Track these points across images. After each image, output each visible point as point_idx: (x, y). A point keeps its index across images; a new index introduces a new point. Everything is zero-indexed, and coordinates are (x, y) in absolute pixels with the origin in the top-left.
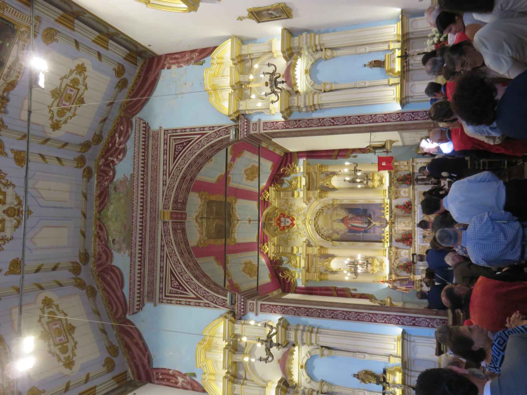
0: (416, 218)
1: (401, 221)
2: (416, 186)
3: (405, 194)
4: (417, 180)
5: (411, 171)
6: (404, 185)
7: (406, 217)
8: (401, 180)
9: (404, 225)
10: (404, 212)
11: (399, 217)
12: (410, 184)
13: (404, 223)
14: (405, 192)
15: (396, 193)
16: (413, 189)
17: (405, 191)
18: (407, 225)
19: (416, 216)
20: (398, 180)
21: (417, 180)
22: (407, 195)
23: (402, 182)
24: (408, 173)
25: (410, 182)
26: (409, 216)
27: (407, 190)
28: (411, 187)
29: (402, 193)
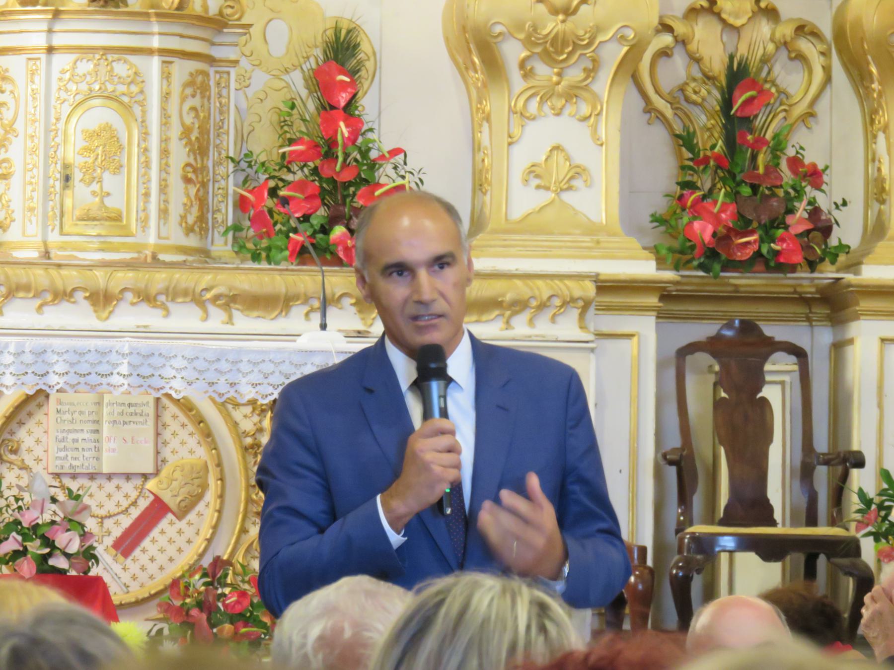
0: (184, 317)
1: (127, 104)
2: (644, 336)
3: (533, 172)
4: (741, 356)
5: (872, 273)
6: (661, 172)
7: (196, 176)
8: (736, 124)
9: (72, 151)
10: (265, 145)
11: (198, 86)
12: (680, 253)
13: (108, 149)
14: (559, 176)
15: (555, 50)
16: (606, 287)
17: (578, 171)
18: (82, 195)
19: (216, 320)
20: (738, 75)
21: (741, 356)
22: (523, 201)
23: (711, 139)
24: (848, 231)
25: (714, 256)
26: (201, 225)
27: (598, 200)
28: (645, 268)
29: (546, 133)
